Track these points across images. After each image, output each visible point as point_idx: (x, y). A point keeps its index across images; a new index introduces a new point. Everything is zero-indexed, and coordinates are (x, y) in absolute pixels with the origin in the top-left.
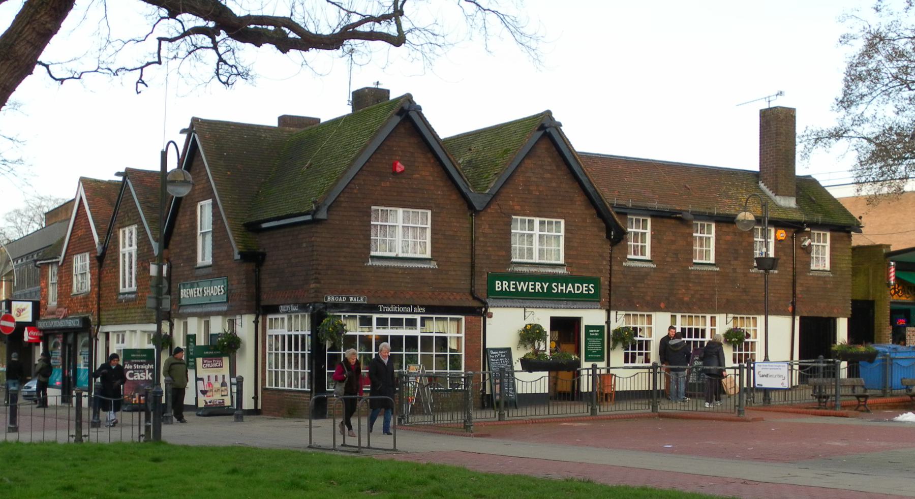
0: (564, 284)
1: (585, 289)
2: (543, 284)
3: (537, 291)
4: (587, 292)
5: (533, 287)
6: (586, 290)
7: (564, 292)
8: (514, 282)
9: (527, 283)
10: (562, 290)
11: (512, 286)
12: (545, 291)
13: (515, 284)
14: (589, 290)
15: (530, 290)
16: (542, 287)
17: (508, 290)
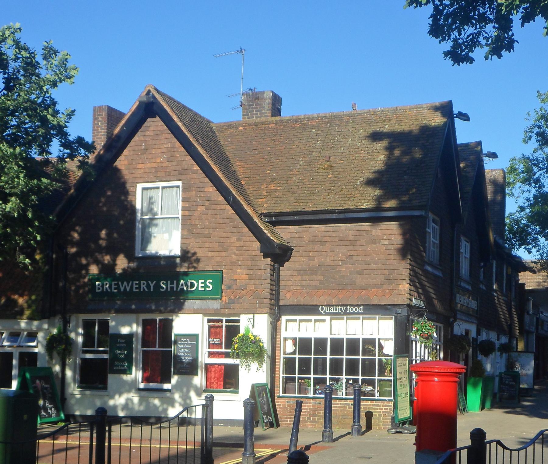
0: (175, 281)
1: (200, 285)
2: (150, 282)
3: (142, 290)
4: (203, 289)
5: (137, 286)
6: (202, 287)
7: (175, 290)
8: (116, 282)
9: (131, 282)
10: (172, 288)
11: (113, 287)
12: (152, 290)
13: (118, 284)
14: (206, 286)
15: (135, 290)
16: (148, 286)
17: (109, 290)
